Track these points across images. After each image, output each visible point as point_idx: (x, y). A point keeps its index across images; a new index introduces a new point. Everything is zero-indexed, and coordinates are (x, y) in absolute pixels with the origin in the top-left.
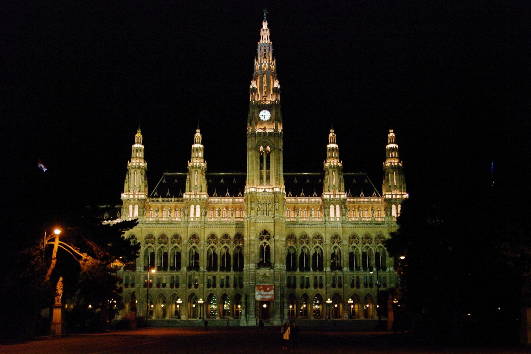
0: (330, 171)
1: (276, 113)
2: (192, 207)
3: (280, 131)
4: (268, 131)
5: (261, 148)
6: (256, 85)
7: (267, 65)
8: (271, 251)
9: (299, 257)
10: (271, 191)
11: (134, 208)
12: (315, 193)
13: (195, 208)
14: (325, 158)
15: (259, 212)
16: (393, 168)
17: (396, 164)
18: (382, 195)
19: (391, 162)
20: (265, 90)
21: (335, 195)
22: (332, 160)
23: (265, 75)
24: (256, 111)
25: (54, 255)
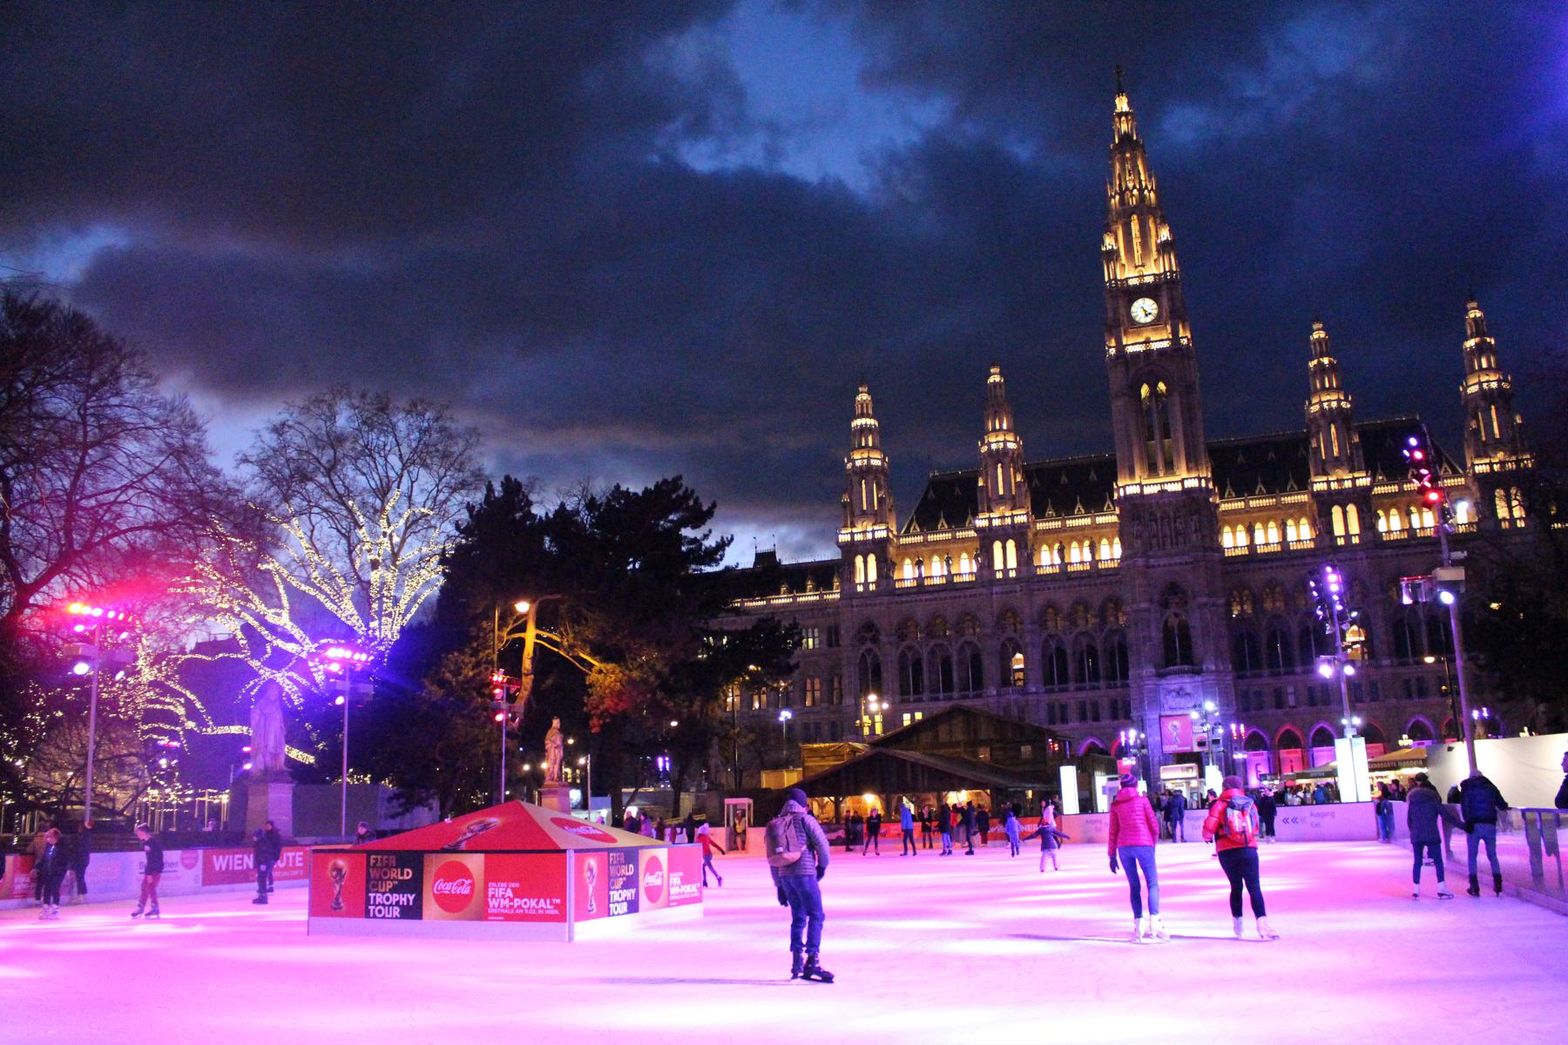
0: (1322, 422)
1: (1171, 299)
2: (997, 546)
3: (1184, 341)
4: (1154, 346)
5: (1145, 390)
6: (1116, 240)
7: (1135, 192)
8: (1192, 632)
9: (1264, 641)
10: (1177, 487)
11: (865, 562)
12: (1291, 482)
13: (1004, 549)
14: (1308, 394)
15: (1154, 541)
16: (1486, 396)
17: (1494, 385)
18: (1464, 467)
19: (1480, 383)
20: (1137, 248)
21: (1340, 481)
22: (1324, 398)
23: (1135, 217)
24: (1121, 303)
25: (527, 664)
